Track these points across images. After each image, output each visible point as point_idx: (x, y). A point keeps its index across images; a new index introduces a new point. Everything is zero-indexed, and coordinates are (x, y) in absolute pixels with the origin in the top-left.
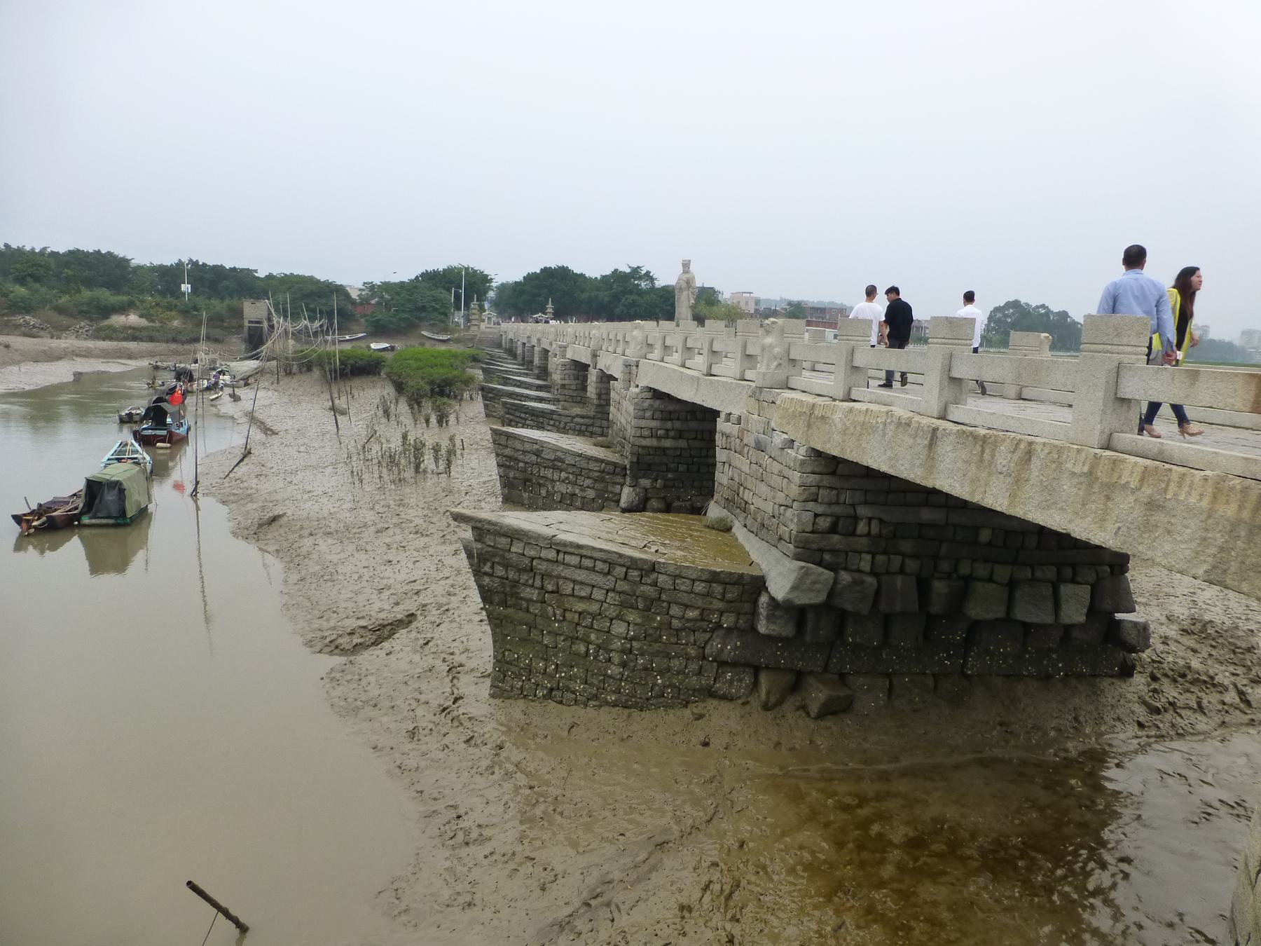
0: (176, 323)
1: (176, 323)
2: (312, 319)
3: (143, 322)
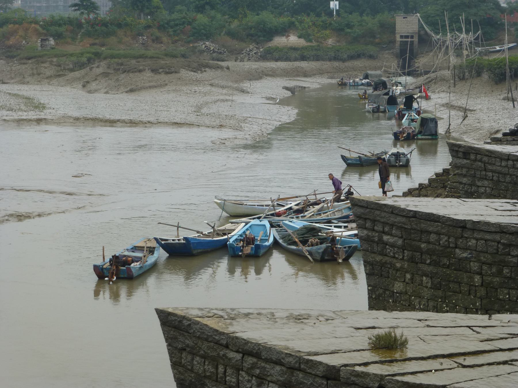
0: (330, 42)
1: (330, 42)
2: (467, 32)
3: (302, 42)
